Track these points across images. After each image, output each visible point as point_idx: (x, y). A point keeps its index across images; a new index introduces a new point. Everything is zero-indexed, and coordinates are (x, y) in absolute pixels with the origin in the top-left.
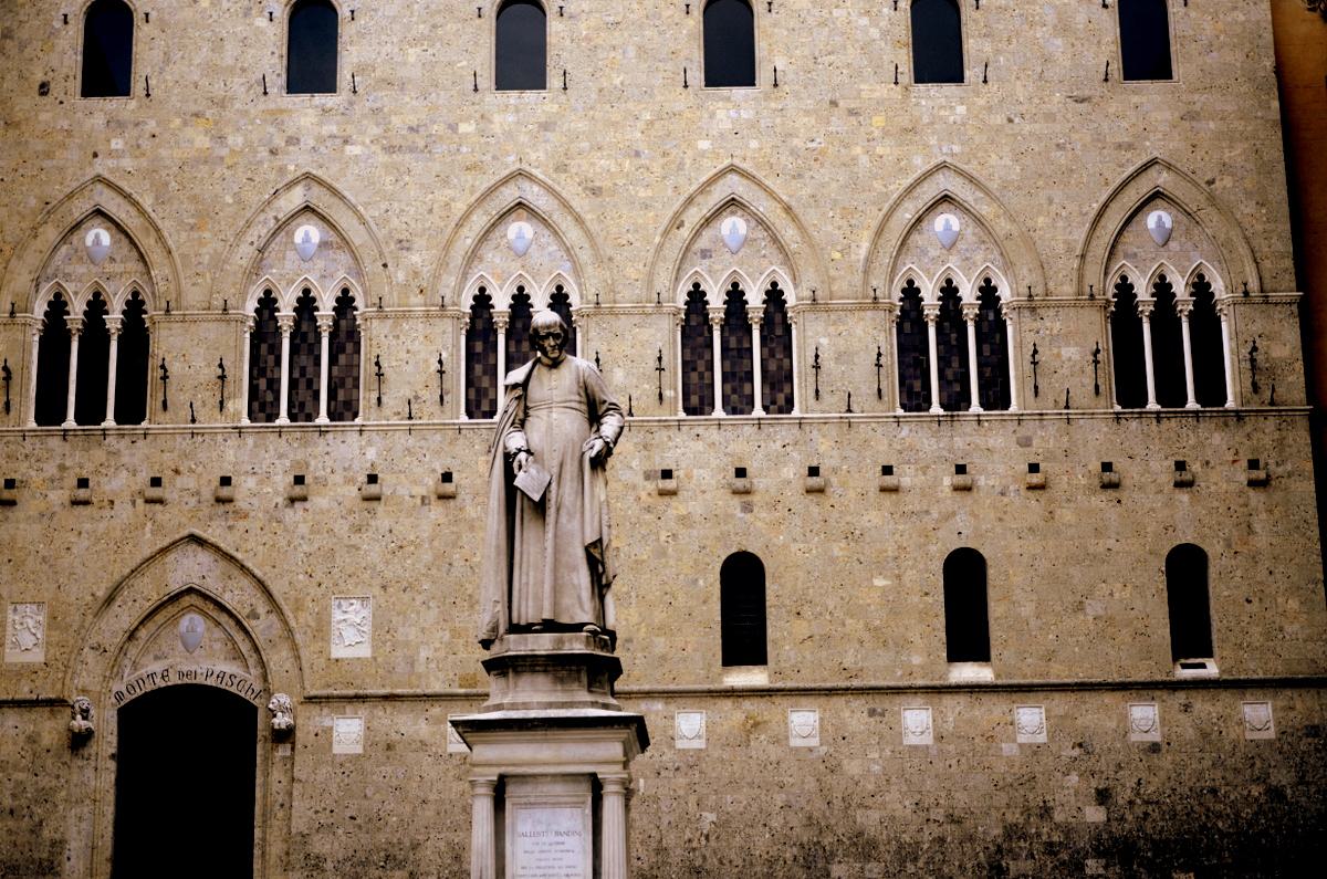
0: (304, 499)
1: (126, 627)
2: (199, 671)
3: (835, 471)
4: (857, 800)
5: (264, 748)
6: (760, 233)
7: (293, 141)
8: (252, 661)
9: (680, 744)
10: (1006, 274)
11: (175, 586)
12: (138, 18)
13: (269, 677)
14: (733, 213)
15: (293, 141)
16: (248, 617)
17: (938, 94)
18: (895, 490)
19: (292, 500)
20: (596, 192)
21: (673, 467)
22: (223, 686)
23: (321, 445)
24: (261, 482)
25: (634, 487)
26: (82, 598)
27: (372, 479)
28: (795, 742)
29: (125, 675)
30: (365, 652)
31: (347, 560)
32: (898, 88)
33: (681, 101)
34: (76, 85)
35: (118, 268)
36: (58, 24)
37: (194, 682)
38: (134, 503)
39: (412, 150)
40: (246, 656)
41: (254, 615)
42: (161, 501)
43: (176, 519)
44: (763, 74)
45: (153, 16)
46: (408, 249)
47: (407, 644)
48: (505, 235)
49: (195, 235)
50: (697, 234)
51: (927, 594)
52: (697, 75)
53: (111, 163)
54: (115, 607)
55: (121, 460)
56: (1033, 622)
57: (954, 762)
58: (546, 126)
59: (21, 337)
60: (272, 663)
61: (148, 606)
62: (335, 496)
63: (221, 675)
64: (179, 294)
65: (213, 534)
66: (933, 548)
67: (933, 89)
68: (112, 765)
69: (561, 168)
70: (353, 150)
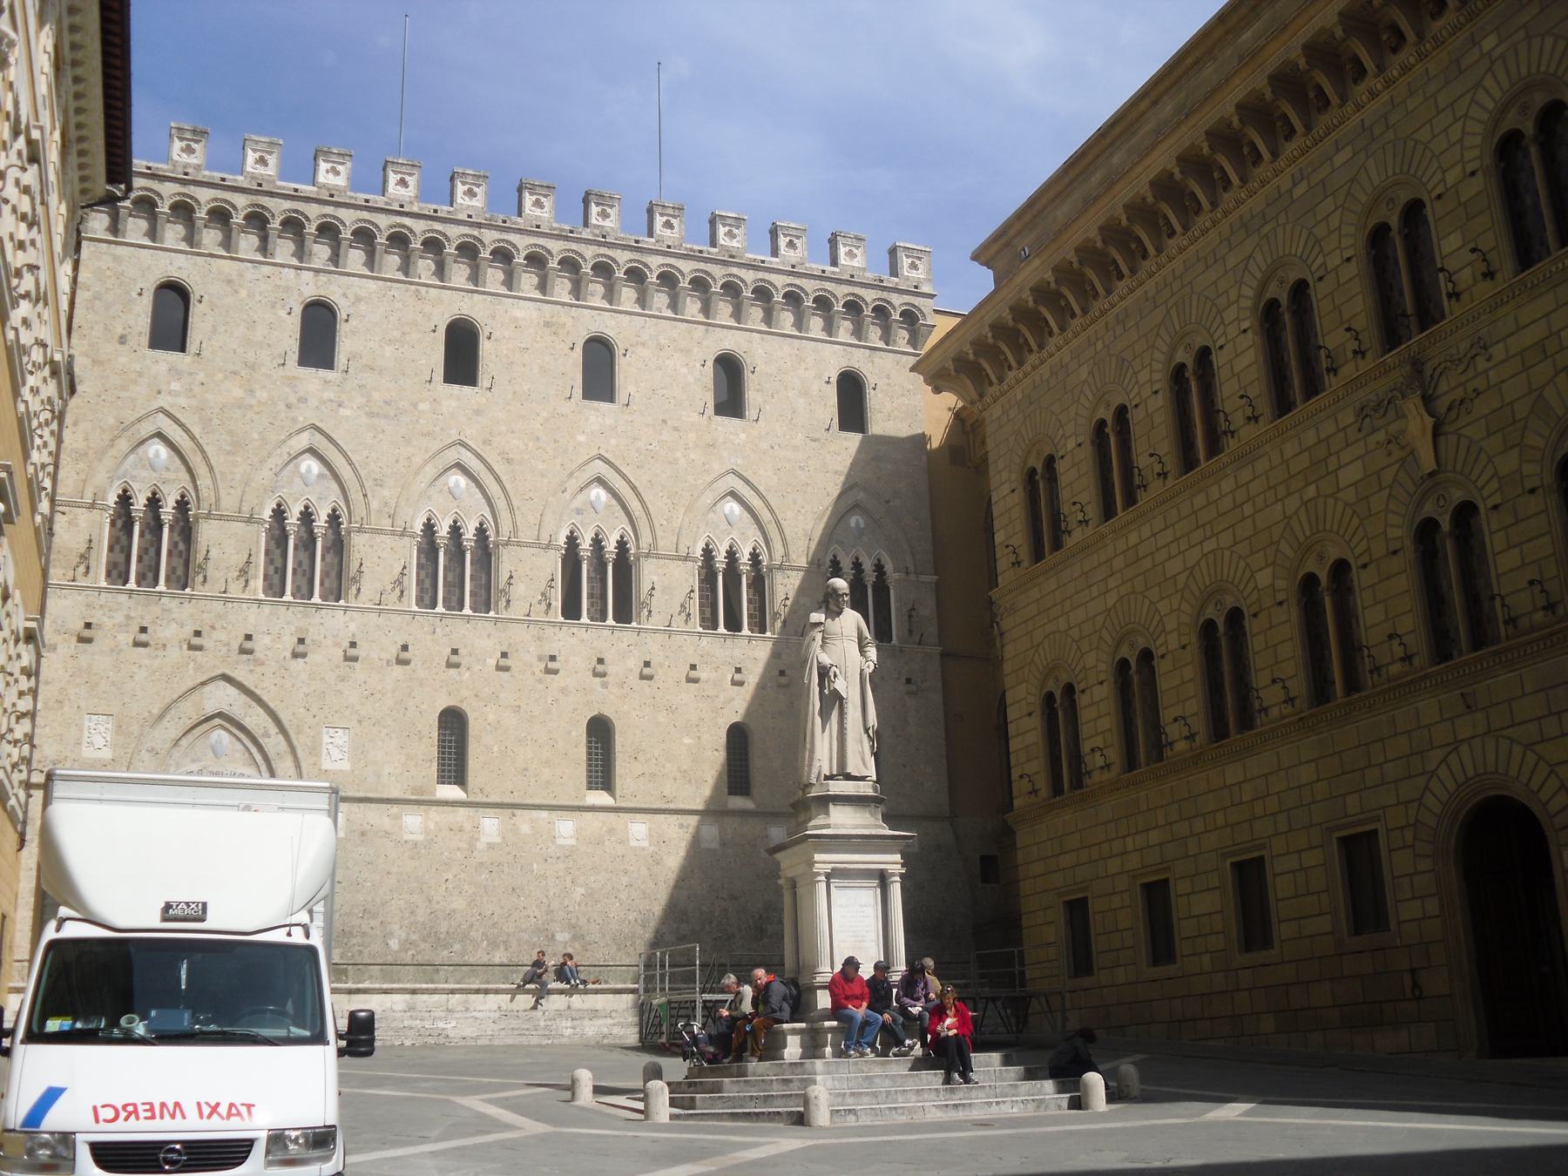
0: (304, 655)
3: (661, 665)
6: (614, 502)
7: (302, 400)
9: (560, 841)
11: (210, 711)
15: (302, 400)
17: (728, 423)
18: (696, 681)
19: (295, 655)
20: (509, 461)
23: (317, 617)
24: (273, 641)
27: (353, 645)
28: (633, 843)
30: (345, 765)
33: (566, 408)
34: (145, 340)
36: (134, 295)
39: (386, 417)
42: (199, 648)
43: (211, 662)
44: (621, 396)
45: (206, 298)
50: (574, 497)
52: (579, 391)
53: (169, 399)
55: (173, 615)
58: (478, 412)
59: (98, 518)
61: (190, 723)
62: (325, 655)
64: (218, 500)
65: (237, 674)
66: (720, 721)
67: (726, 420)
69: (487, 442)
70: (344, 412)
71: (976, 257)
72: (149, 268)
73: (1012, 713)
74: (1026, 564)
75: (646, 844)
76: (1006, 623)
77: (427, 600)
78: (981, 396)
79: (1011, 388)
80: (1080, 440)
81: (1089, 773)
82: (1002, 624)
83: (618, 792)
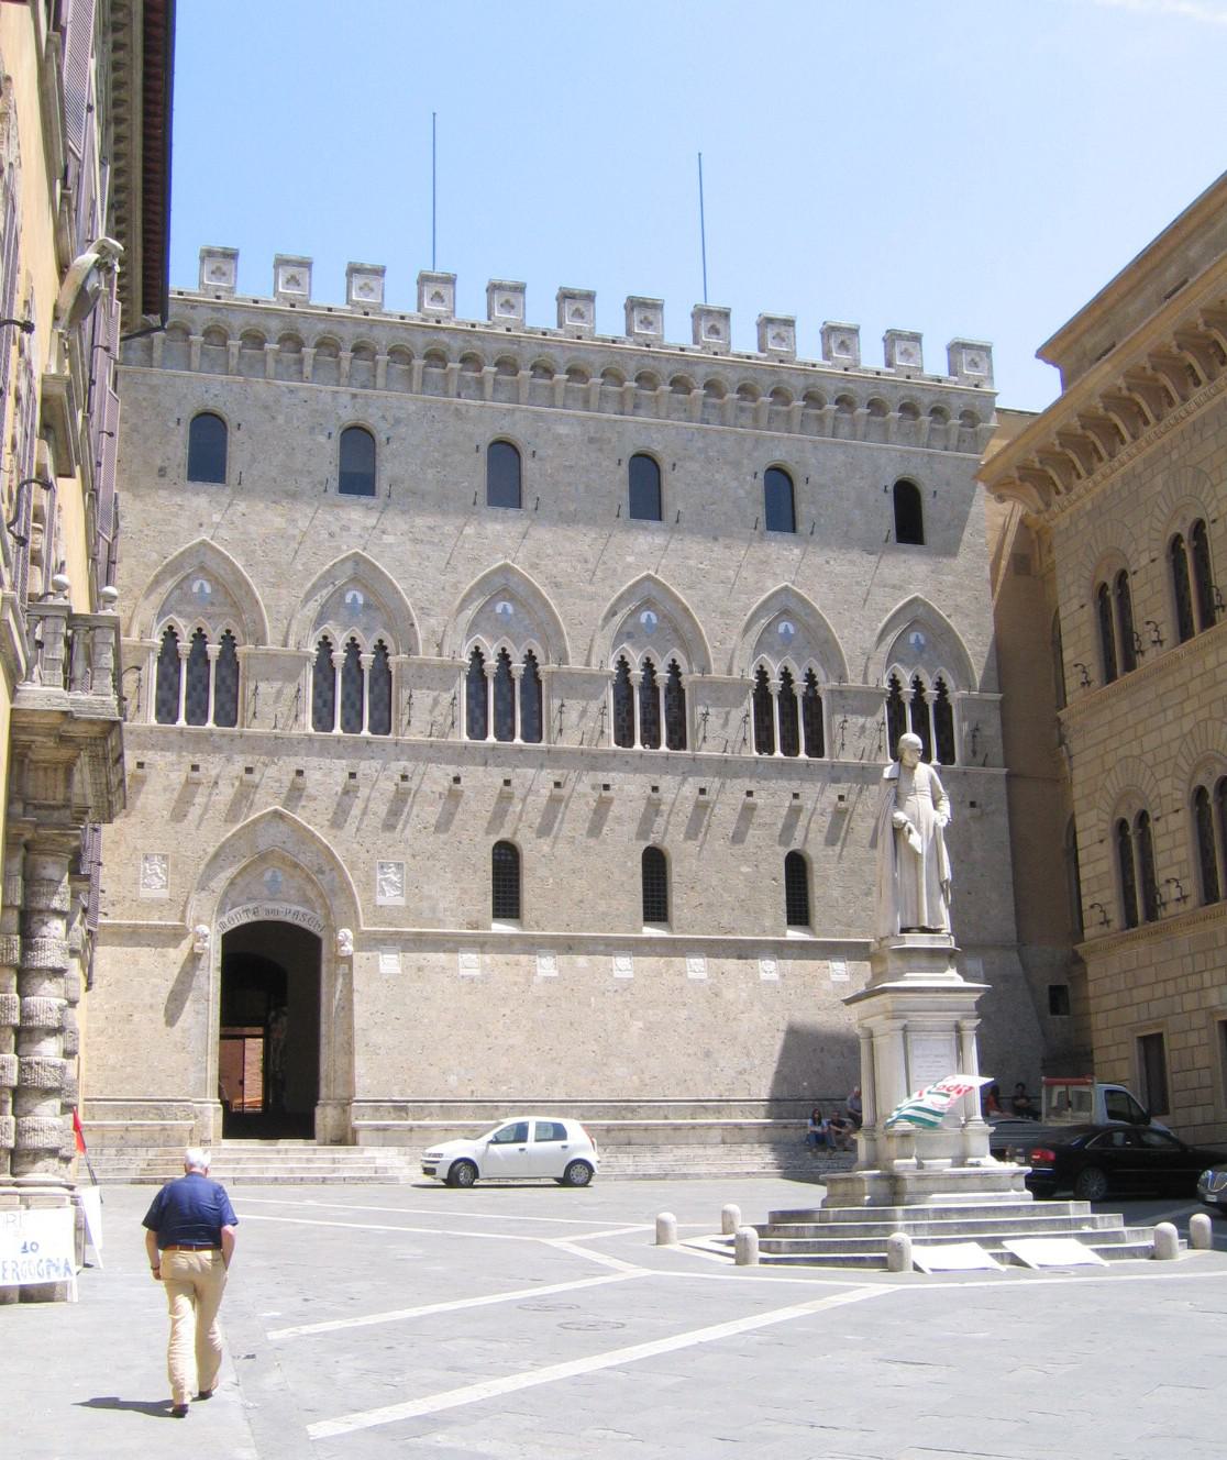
4: (732, 1017)
9: (617, 974)
10: (822, 666)
12: (231, 427)
14: (648, 609)
15: (345, 528)
20: (557, 585)
21: (611, 783)
24: (325, 775)
25: (585, 795)
28: (691, 975)
30: (401, 901)
32: (757, 532)
34: (184, 472)
35: (217, 610)
36: (172, 425)
41: (321, 871)
44: (669, 513)
46: (428, 615)
47: (429, 897)
48: (494, 610)
49: (275, 591)
51: (774, 879)
52: (626, 510)
56: (841, 902)
57: (793, 992)
68: (219, 975)
70: (388, 539)
71: (1040, 354)
72: (185, 396)
73: (1082, 840)
74: (1096, 683)
75: (704, 976)
76: (1076, 745)
77: (477, 731)
78: (1048, 505)
79: (1079, 497)
80: (1154, 554)
81: (1164, 904)
82: (1070, 745)
83: (675, 924)
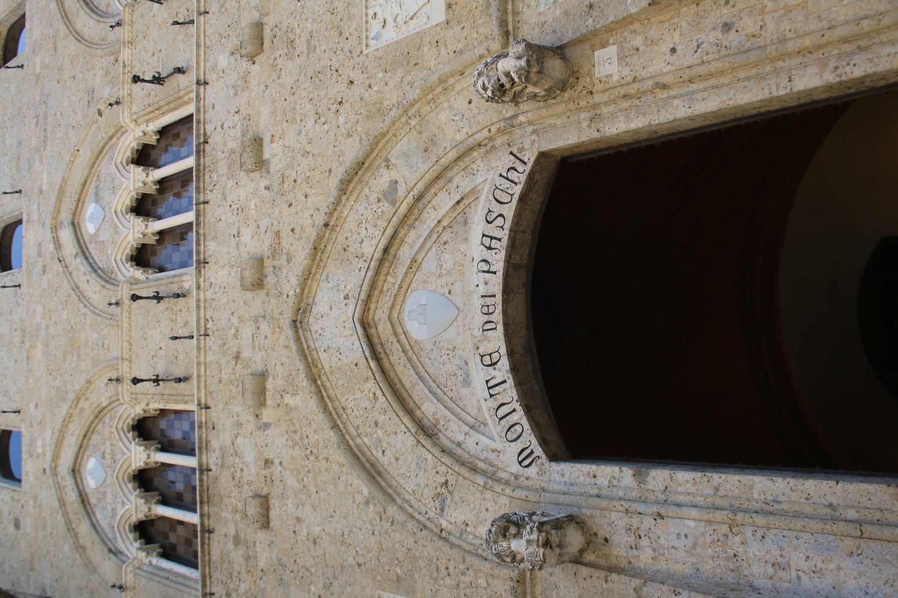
1: (411, 441)
2: (482, 290)
5: (613, 116)
8: (462, 183)
13: (479, 137)
16: (393, 203)
22: (504, 235)
26: (371, 522)
29: (493, 445)
31: (323, 48)
37: (499, 298)
38: (267, 426)
40: (458, 198)
54: (385, 460)
60: (459, 137)
63: (487, 241)
68: (659, 477)
